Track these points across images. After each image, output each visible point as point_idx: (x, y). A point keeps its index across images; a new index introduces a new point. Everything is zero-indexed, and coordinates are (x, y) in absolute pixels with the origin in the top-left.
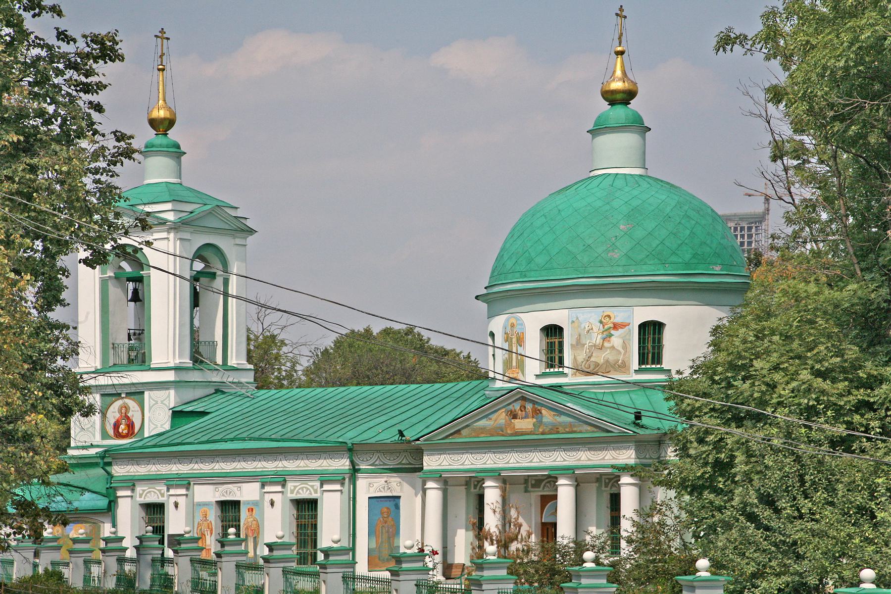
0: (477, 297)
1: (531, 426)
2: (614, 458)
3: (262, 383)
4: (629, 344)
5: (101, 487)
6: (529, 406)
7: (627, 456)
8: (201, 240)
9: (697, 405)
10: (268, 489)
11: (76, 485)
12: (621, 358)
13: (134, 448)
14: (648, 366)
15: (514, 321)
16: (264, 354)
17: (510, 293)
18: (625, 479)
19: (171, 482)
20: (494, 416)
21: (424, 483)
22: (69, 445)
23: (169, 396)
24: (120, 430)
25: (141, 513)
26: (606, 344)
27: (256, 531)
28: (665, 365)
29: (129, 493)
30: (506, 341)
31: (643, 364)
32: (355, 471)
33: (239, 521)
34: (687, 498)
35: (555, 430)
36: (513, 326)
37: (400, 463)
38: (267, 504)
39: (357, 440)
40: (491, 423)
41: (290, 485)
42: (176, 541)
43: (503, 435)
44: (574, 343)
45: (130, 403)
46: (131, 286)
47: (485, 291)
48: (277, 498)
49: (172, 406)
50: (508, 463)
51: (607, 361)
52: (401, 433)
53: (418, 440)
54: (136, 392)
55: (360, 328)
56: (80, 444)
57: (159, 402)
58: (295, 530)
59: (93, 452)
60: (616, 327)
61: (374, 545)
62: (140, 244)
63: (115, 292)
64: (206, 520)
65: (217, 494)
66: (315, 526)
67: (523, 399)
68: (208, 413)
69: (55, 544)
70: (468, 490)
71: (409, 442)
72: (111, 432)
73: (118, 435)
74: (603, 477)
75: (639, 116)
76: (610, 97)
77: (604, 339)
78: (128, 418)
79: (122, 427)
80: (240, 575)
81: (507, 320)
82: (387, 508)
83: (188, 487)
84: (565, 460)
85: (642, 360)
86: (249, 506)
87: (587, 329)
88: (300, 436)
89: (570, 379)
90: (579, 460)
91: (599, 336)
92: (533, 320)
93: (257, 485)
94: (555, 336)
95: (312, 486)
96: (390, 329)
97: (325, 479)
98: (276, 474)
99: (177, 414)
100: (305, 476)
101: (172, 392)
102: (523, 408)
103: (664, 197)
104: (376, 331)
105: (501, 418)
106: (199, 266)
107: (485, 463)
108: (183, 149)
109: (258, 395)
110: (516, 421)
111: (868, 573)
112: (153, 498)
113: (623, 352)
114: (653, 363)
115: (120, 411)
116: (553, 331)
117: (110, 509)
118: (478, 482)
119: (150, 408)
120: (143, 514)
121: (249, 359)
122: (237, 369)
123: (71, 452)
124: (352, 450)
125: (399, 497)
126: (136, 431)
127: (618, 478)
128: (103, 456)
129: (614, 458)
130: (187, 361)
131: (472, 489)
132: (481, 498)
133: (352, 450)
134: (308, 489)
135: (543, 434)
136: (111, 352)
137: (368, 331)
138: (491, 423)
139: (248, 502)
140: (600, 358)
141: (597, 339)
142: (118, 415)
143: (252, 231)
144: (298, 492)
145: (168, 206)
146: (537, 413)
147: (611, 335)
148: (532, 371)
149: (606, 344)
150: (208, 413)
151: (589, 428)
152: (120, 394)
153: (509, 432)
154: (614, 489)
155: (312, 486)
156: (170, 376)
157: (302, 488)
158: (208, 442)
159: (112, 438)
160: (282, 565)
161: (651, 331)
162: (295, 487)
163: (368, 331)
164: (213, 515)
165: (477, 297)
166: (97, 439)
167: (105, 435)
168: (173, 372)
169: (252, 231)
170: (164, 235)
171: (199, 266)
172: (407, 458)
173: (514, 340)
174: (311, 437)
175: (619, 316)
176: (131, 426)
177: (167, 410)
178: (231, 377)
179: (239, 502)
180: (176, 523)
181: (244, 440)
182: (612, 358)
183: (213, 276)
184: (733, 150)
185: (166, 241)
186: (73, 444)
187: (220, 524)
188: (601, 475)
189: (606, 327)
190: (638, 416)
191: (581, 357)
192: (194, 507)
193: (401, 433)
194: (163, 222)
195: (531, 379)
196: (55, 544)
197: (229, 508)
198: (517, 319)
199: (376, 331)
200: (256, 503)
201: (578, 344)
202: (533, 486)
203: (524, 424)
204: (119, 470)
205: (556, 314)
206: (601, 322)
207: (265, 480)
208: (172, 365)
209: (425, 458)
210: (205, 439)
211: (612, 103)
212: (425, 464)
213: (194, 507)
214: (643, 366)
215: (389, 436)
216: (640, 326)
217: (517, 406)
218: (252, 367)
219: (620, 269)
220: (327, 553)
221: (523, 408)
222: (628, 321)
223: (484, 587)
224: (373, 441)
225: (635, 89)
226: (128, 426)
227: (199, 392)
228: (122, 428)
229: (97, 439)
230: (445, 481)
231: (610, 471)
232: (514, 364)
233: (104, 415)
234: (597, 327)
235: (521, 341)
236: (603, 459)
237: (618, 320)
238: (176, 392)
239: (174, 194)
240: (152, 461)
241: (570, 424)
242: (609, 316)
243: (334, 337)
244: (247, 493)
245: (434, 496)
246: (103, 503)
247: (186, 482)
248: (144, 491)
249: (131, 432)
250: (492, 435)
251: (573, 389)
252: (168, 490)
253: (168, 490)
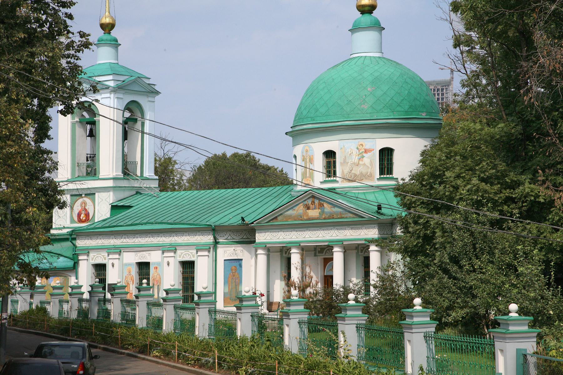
0: (286, 133)
1: (318, 214)
2: (366, 234)
3: (163, 187)
4: (373, 162)
5: (69, 254)
6: (317, 202)
7: (373, 233)
8: (129, 98)
9: (413, 200)
10: (166, 254)
11: (55, 252)
12: (369, 171)
13: (89, 229)
14: (385, 176)
16: (165, 170)
17: (305, 131)
18: (373, 248)
19: (111, 250)
20: (296, 208)
21: (256, 251)
22: (51, 227)
24: (81, 218)
25: (92, 270)
26: (361, 162)
27: (159, 282)
28: (395, 175)
29: (85, 257)
30: (303, 160)
31: (382, 174)
32: (216, 243)
33: (149, 275)
34: (408, 259)
35: (331, 216)
36: (307, 151)
38: (166, 264)
39: (217, 224)
40: (295, 212)
41: (179, 252)
42: (113, 288)
43: (301, 220)
44: (342, 162)
45: (87, 200)
46: (89, 127)
47: (291, 130)
48: (171, 260)
49: (111, 202)
50: (304, 237)
51: (361, 173)
52: (243, 219)
53: (252, 223)
54: (91, 194)
55: (219, 153)
56: (57, 227)
58: (181, 281)
59: (65, 231)
60: (366, 151)
61: (227, 290)
62: (93, 100)
63: (79, 131)
64: (130, 275)
65: (137, 258)
66: (193, 278)
67: (313, 197)
68: (132, 207)
69: (42, 290)
70: (281, 255)
71: (248, 224)
72: (76, 219)
73: (80, 221)
74: (360, 246)
75: (378, 20)
76: (361, 9)
77: (359, 159)
78: (86, 210)
79: (82, 215)
80: (149, 310)
81: (304, 147)
82: (234, 266)
83: (120, 253)
84: (337, 236)
85: (382, 172)
86: (156, 266)
87: (349, 153)
88: (185, 221)
89: (340, 184)
90: (346, 235)
91: (357, 157)
92: (318, 147)
93: (160, 252)
94: (331, 157)
95: (191, 253)
96: (237, 153)
97: (199, 248)
98: (171, 245)
99: (114, 208)
100: (189, 247)
101: (111, 193)
102: (313, 203)
103: (392, 71)
104: (229, 155)
105: (300, 209)
106: (127, 114)
107: (291, 238)
108: (119, 42)
109: (161, 195)
110: (309, 211)
111: (513, 307)
112: (100, 261)
113: (370, 167)
114: (388, 174)
115: (81, 205)
116: (330, 155)
117: (74, 268)
118: (288, 250)
119: (99, 204)
120: (94, 271)
121: (156, 173)
122: (149, 179)
123: (52, 232)
124: (215, 230)
125: (242, 260)
126: (90, 218)
127: (368, 247)
128: (71, 234)
129: (366, 234)
130: (120, 174)
131: (284, 255)
132: (289, 260)
133: (215, 230)
134: (189, 255)
135: (324, 219)
136: (77, 168)
137: (224, 155)
138: (295, 212)
139: (154, 263)
140: (357, 171)
141: (355, 159)
142: (80, 208)
143: (158, 93)
144: (183, 257)
145: (111, 77)
146: (321, 206)
147: (363, 157)
148: (318, 180)
149: (361, 162)
150: (132, 207)
151: (351, 215)
152: (81, 195)
153: (305, 218)
154: (366, 254)
155: (191, 253)
156: (110, 183)
157: (186, 254)
158: (131, 225)
159: (76, 223)
160: (174, 303)
161: (386, 155)
162: (182, 253)
163: (224, 155)
164: (134, 271)
165: (286, 133)
167: (72, 221)
168: (112, 181)
169: (158, 93)
170: (108, 95)
171: (127, 114)
172: (245, 234)
173: (308, 160)
174: (191, 222)
175: (368, 144)
176: (87, 215)
177: (108, 204)
178: (146, 184)
179: (149, 263)
180: (112, 277)
181: (152, 223)
182: (364, 171)
183: (135, 121)
184: (428, 42)
185: (109, 99)
186: (54, 227)
187: (138, 277)
188: (359, 245)
189: (361, 151)
190: (379, 207)
191: (346, 171)
192: (123, 265)
193: (243, 219)
194: (108, 88)
195: (317, 184)
196: (42, 290)
197: (143, 267)
198: (310, 147)
199: (229, 155)
200: (159, 264)
201: (344, 162)
202: (320, 252)
203: (314, 213)
204: (81, 243)
205: (331, 143)
206: (357, 148)
207: (164, 249)
208: (111, 176)
209: (257, 235)
210: (130, 223)
211: (363, 13)
213: (123, 265)
214: (382, 176)
215: (236, 221)
216: (380, 151)
217: (309, 202)
218: (157, 177)
219: (368, 115)
220: (200, 296)
221: (313, 203)
222: (373, 148)
223: (291, 317)
224: (226, 224)
225: (375, 4)
226: (86, 215)
227: (127, 194)
228: (83, 216)
229: (68, 223)
230: (269, 250)
231: (363, 242)
232: (308, 175)
233: (72, 208)
234: (355, 151)
235: (311, 161)
236: (360, 235)
237: (367, 147)
238: (113, 193)
239: (115, 70)
240: (100, 237)
241: (341, 213)
242: (362, 145)
243: (205, 159)
244: (153, 257)
245: (262, 259)
246: (70, 264)
247: (119, 250)
248: (94, 256)
249: (87, 219)
250: (295, 220)
251: (341, 191)
252: (108, 255)
253: (108, 255)
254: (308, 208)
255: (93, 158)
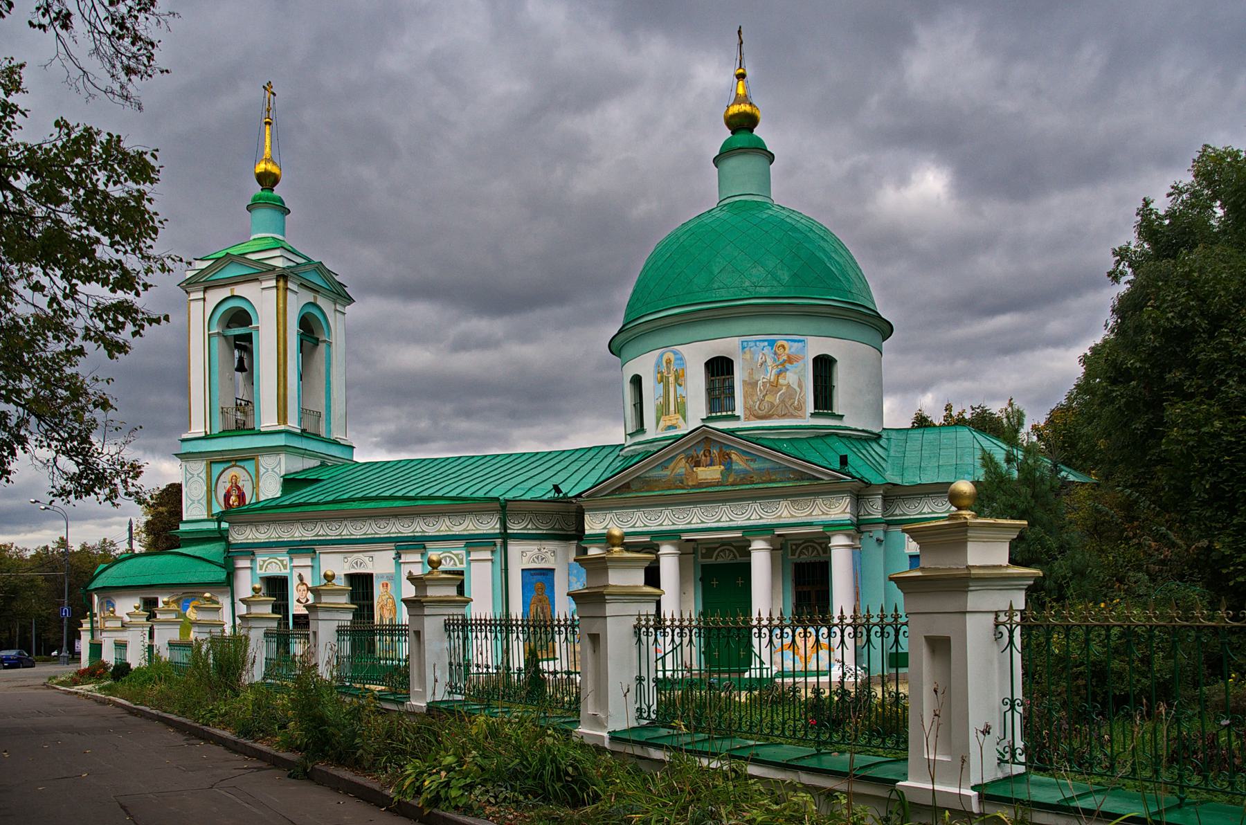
23: (279, 463)
78: (239, 488)
81: (661, 356)
92: (694, 355)
95: (457, 555)
97: (473, 542)
101: (283, 457)
116: (719, 368)
134: (451, 559)
142: (228, 485)
155: (457, 555)
156: (280, 441)
175: (792, 348)
186: (184, 519)
226: (238, 496)
246: (221, 575)
255: (246, 406)
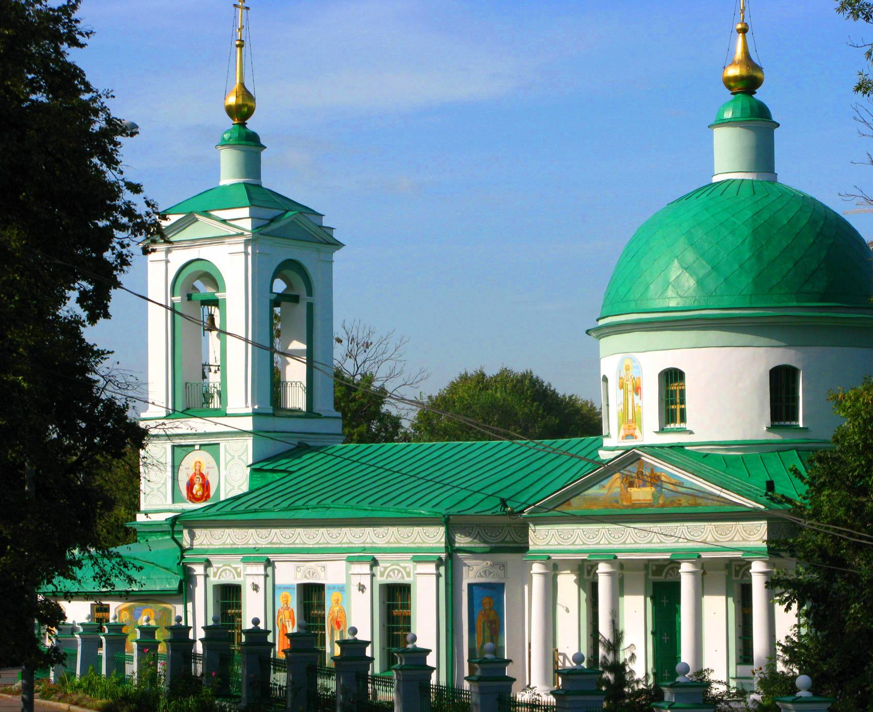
0: (587, 332)
1: (649, 497)
15: (628, 362)
20: (607, 483)
24: (194, 491)
36: (627, 368)
37: (503, 541)
38: (354, 589)
52: (504, 503)
57: (236, 457)
68: (291, 473)
72: (184, 492)
73: (193, 498)
78: (202, 476)
81: (622, 361)
95: (405, 568)
107: (598, 543)
116: (672, 378)
128: (174, 521)
134: (399, 571)
142: (191, 472)
144: (388, 575)
152: (193, 446)
153: (625, 503)
157: (393, 570)
166: (168, 503)
173: (630, 387)
176: (206, 486)
198: (634, 360)
207: (354, 556)
212: (530, 543)
228: (197, 489)
249: (205, 496)
254: (631, 485)
